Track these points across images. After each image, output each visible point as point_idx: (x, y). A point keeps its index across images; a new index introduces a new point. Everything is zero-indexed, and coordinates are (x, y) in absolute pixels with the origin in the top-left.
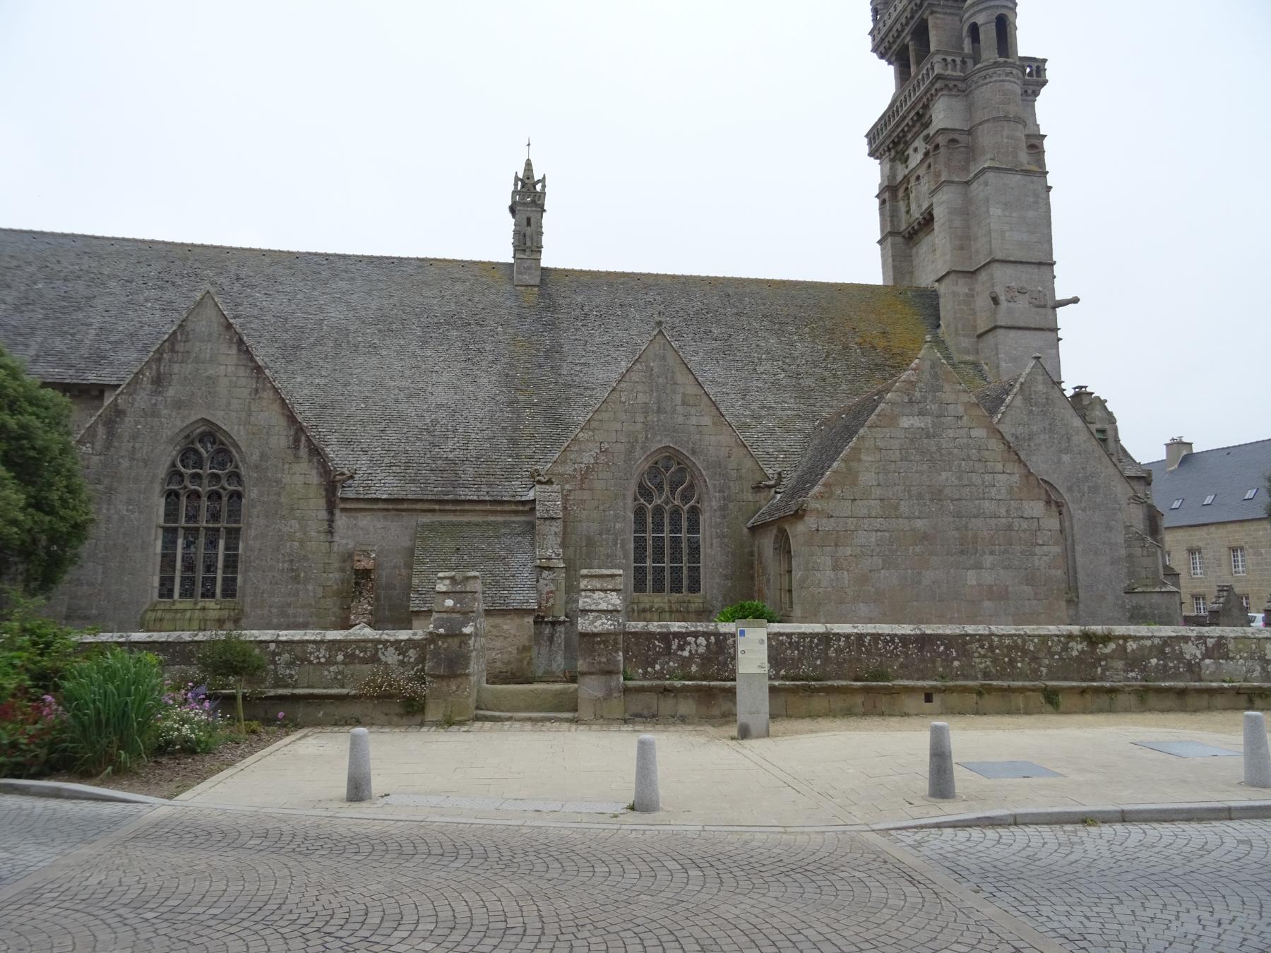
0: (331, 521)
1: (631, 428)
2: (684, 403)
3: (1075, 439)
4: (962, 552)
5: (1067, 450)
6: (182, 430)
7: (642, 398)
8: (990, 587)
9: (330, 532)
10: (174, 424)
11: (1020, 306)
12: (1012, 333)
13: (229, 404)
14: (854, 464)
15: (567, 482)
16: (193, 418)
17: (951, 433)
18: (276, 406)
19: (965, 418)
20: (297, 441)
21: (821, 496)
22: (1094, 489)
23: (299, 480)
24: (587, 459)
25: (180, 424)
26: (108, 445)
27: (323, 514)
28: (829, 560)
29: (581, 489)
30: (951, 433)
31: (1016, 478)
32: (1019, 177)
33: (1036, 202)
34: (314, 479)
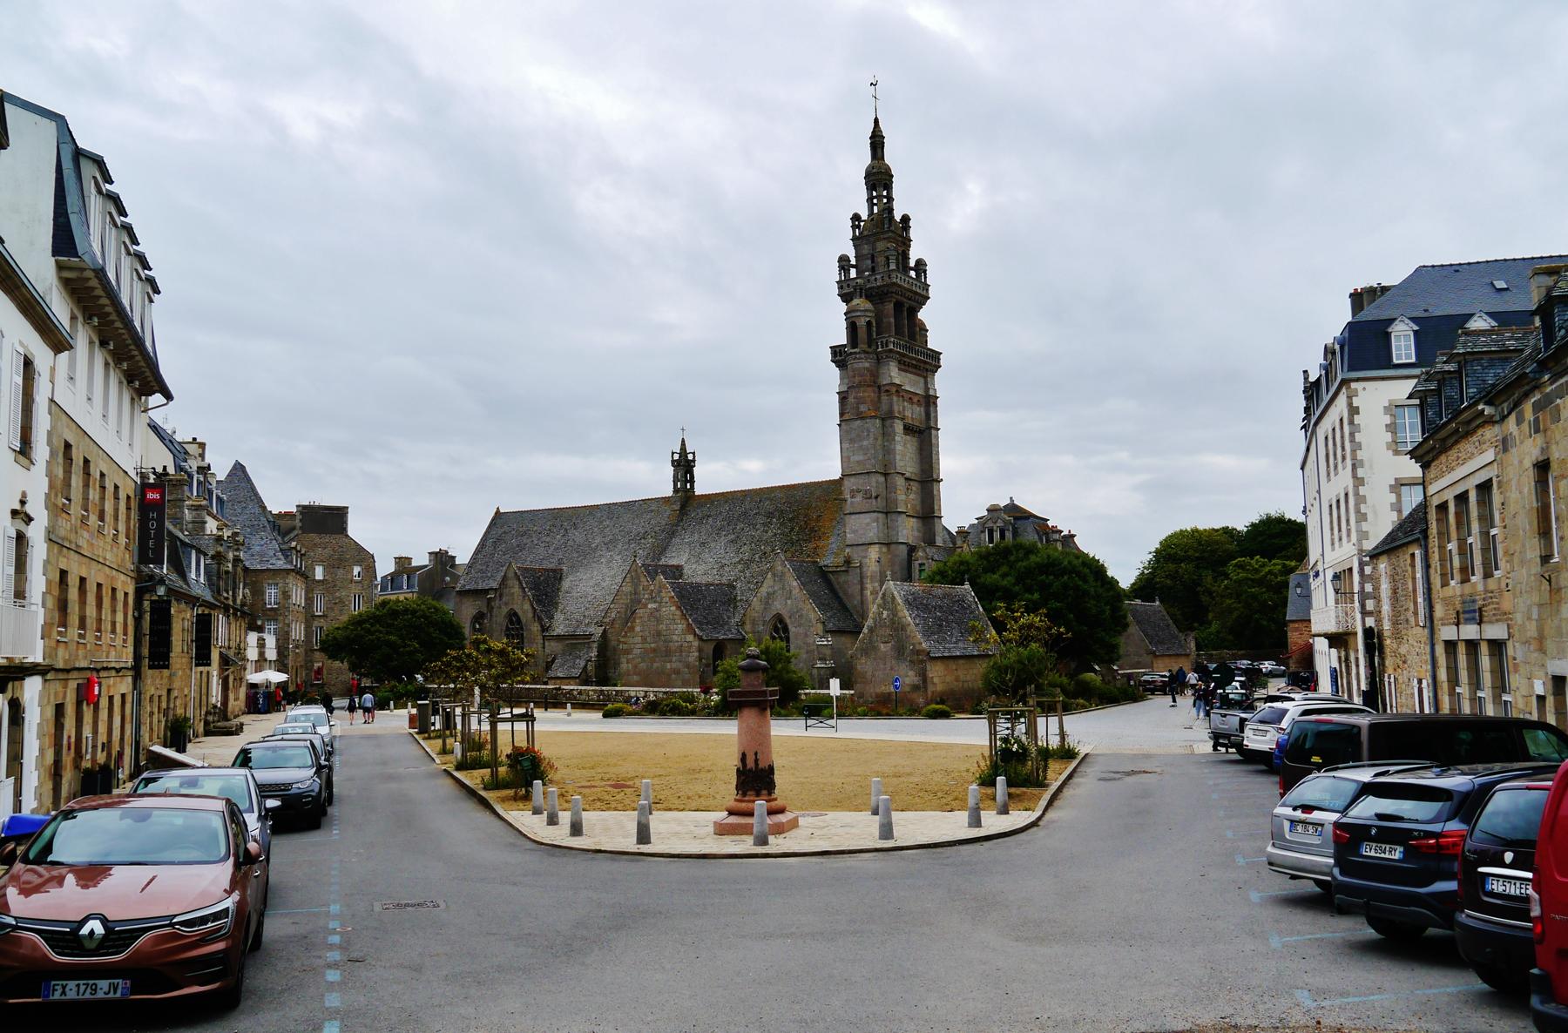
0: (544, 643)
2: (643, 589)
3: (794, 592)
4: (666, 656)
7: (630, 589)
9: (544, 648)
10: (505, 610)
12: (853, 517)
22: (801, 616)
23: (536, 629)
24: (613, 615)
25: (506, 611)
27: (542, 641)
32: (859, 422)
33: (868, 435)
34: (539, 628)
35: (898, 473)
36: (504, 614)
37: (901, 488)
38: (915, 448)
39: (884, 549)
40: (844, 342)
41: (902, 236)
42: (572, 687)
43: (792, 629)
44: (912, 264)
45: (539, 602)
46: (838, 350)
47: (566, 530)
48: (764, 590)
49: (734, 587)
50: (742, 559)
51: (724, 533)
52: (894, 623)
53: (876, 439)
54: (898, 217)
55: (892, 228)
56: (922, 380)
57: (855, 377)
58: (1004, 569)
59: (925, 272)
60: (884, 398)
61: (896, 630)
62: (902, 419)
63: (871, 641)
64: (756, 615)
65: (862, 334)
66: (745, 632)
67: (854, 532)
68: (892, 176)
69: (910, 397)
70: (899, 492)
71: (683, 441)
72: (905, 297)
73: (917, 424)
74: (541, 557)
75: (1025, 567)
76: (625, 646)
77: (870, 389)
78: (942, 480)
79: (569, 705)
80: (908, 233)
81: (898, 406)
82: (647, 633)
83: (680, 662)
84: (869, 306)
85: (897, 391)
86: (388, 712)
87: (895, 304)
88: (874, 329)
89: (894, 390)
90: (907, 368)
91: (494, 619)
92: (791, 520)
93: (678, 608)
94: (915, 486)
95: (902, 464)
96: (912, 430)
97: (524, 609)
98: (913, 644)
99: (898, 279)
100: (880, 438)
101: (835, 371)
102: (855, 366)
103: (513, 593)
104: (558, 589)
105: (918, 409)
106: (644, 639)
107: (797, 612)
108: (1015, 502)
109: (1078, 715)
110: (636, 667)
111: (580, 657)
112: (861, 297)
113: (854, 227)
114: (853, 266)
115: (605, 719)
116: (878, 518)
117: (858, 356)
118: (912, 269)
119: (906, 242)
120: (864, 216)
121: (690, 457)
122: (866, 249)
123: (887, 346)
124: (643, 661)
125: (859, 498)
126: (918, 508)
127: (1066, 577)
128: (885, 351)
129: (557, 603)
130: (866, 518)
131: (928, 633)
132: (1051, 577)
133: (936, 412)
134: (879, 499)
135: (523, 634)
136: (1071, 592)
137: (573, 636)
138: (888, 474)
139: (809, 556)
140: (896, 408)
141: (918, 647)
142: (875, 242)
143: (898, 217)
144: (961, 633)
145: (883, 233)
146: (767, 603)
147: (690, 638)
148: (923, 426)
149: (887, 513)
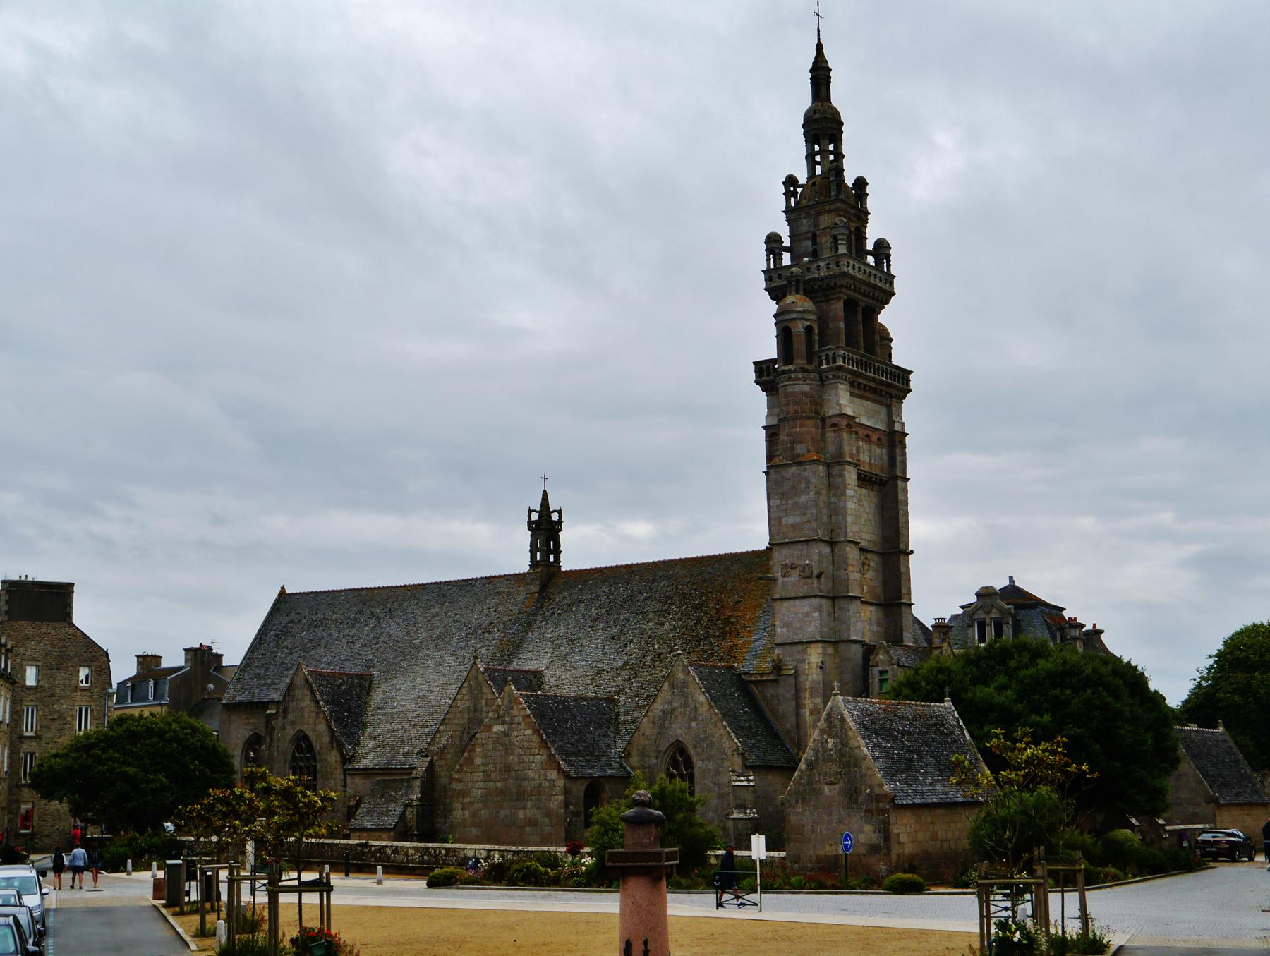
1: (462, 722)
2: (487, 705)
3: (700, 711)
4: (518, 800)
5: (695, 719)
6: (294, 736)
7: (467, 704)
8: (530, 819)
9: (345, 786)
10: (291, 732)
11: (793, 579)
12: (786, 604)
13: (308, 721)
14: (472, 753)
15: (435, 755)
16: (297, 730)
17: (516, 733)
18: (324, 721)
19: (523, 724)
20: (332, 738)
21: (458, 772)
22: (711, 745)
23: (333, 759)
24: (443, 741)
26: (270, 745)
27: (342, 777)
28: (460, 804)
29: (441, 759)
30: (516, 733)
31: (545, 757)
32: (795, 468)
33: (807, 487)
35: (850, 542)
36: (289, 738)
37: (854, 563)
38: (873, 506)
39: (830, 650)
40: (773, 354)
41: (855, 207)
42: (384, 843)
43: (698, 764)
44: (870, 246)
45: (339, 721)
46: (764, 367)
47: (378, 619)
48: (658, 707)
49: (615, 703)
50: (627, 663)
51: (601, 625)
52: (843, 756)
53: (818, 493)
54: (849, 181)
55: (842, 196)
56: (884, 410)
57: (789, 405)
58: (1002, 679)
59: (888, 257)
60: (830, 435)
61: (847, 765)
62: (856, 465)
63: (810, 783)
64: (647, 742)
65: (799, 345)
66: (631, 767)
67: (787, 625)
68: (842, 124)
69: (867, 434)
70: (851, 568)
71: (545, 494)
72: (860, 293)
73: (877, 473)
74: (343, 657)
75: (1030, 677)
76: (460, 786)
77: (810, 422)
78: (912, 552)
79: (379, 868)
80: (864, 202)
81: (850, 446)
82: (491, 767)
83: (538, 808)
84: (809, 305)
85: (848, 425)
86: (123, 875)
87: (844, 302)
88: (817, 338)
89: (844, 423)
90: (861, 393)
91: (276, 744)
92: (697, 608)
93: (536, 731)
94: (874, 561)
95: (856, 528)
96: (870, 481)
97: (318, 731)
98: (871, 787)
99: (850, 266)
100: (824, 492)
101: (760, 398)
102: (790, 389)
103: (302, 709)
104: (366, 703)
105: (878, 450)
106: (487, 778)
107: (706, 738)
108: (1016, 584)
109: (1108, 890)
110: (474, 815)
111: (395, 801)
112: (797, 292)
113: (788, 194)
114: (786, 249)
115: (430, 890)
116: (821, 606)
117: (793, 376)
118: (869, 253)
119: (862, 216)
120: (803, 179)
121: (555, 517)
122: (805, 225)
123: (834, 361)
124: (486, 806)
125: (793, 577)
126: (879, 591)
127: (1089, 691)
128: (832, 369)
129: (364, 723)
130: (804, 606)
131: (891, 770)
132: (1068, 692)
133: (904, 454)
134: (822, 579)
135: (315, 767)
136: (1096, 713)
137: (386, 771)
138: (836, 543)
139: (722, 659)
140: (847, 449)
141: (877, 790)
142: (818, 215)
143: (849, 181)
144: (940, 770)
145: (829, 203)
146: (662, 726)
147: (553, 774)
148: (885, 475)
149: (833, 599)
